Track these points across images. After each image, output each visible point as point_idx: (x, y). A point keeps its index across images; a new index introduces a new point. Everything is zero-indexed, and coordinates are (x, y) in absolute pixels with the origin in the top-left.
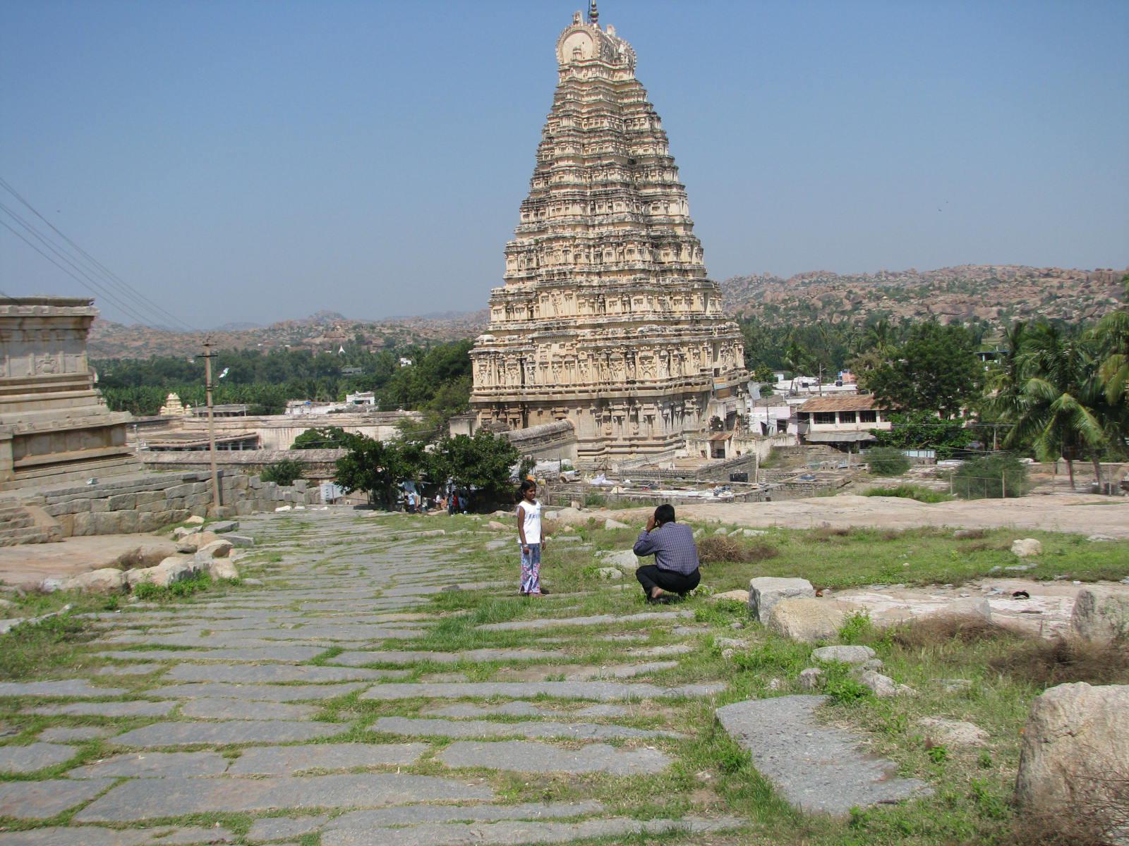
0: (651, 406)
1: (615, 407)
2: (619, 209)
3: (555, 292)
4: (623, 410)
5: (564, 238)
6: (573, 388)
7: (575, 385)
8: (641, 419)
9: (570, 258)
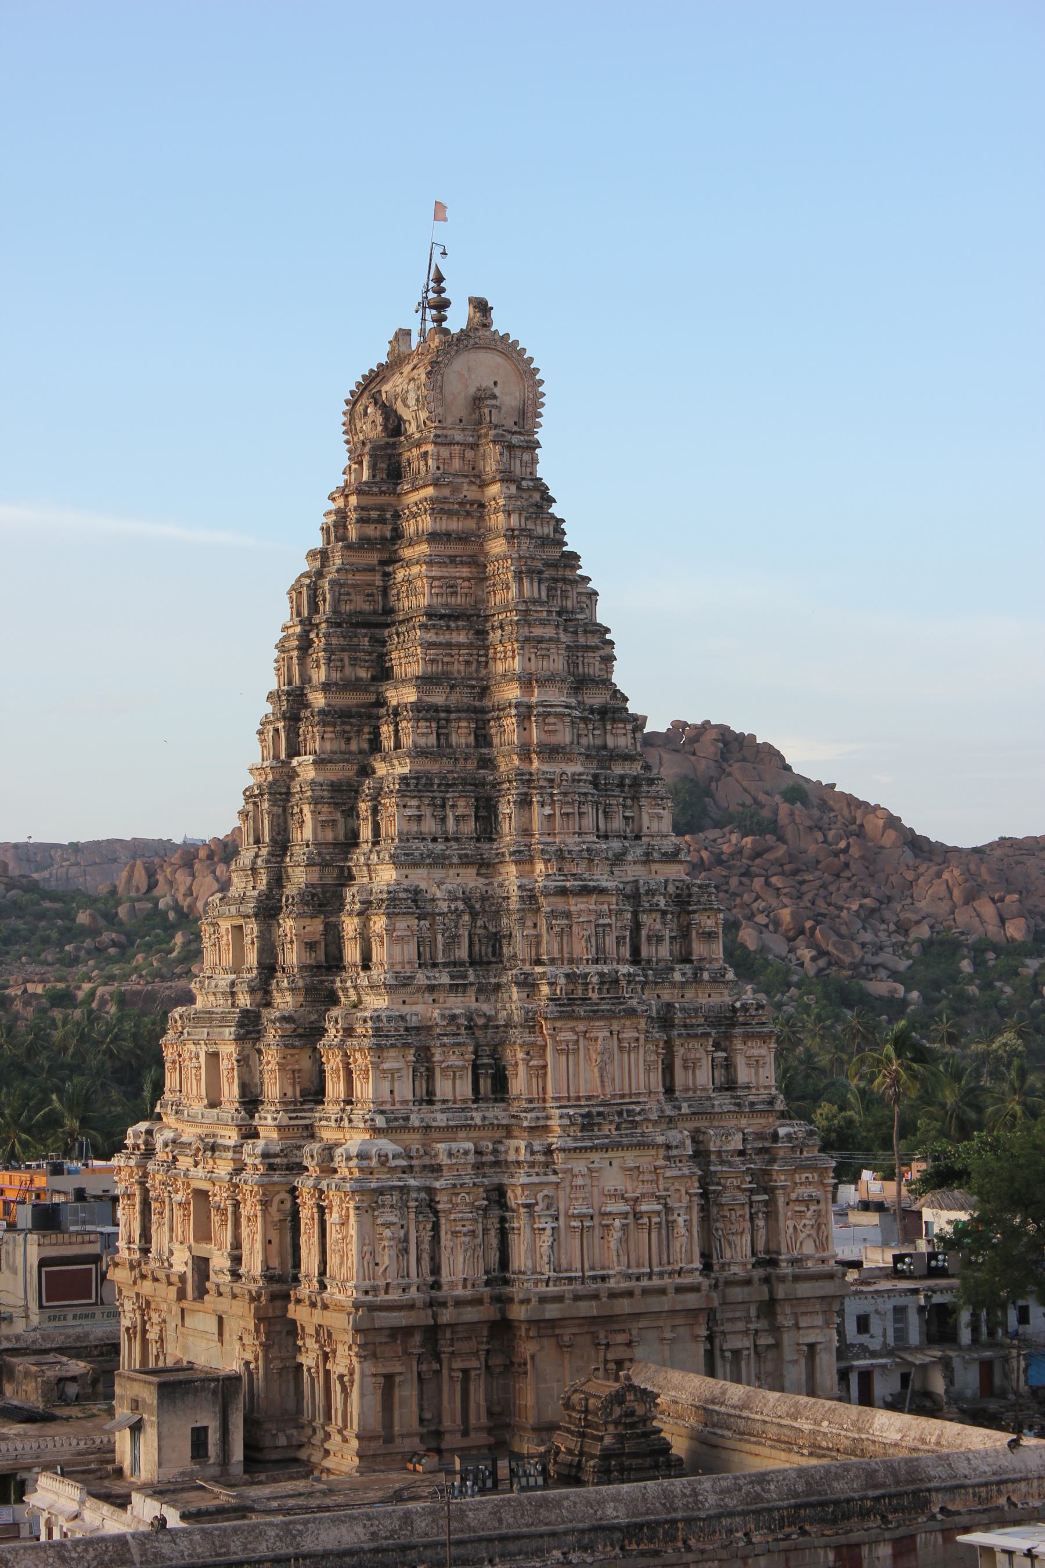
0: (819, 1320)
1: (728, 1327)
2: (655, 826)
4: (746, 1332)
5: (602, 891)
6: (656, 1282)
7: (661, 1275)
8: (789, 1354)
9: (610, 942)
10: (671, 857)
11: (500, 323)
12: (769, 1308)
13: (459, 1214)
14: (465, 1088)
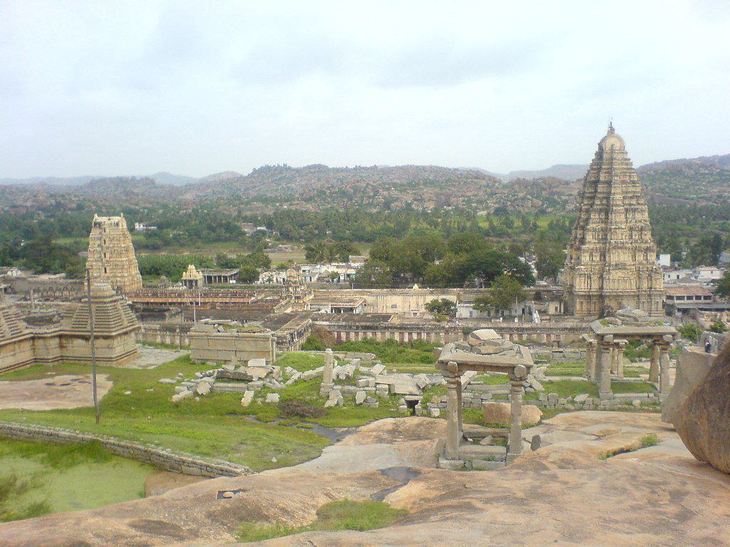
3: (620, 251)
10: (640, 221)
11: (616, 132)
12: (650, 295)
13: (595, 277)
14: (598, 259)
